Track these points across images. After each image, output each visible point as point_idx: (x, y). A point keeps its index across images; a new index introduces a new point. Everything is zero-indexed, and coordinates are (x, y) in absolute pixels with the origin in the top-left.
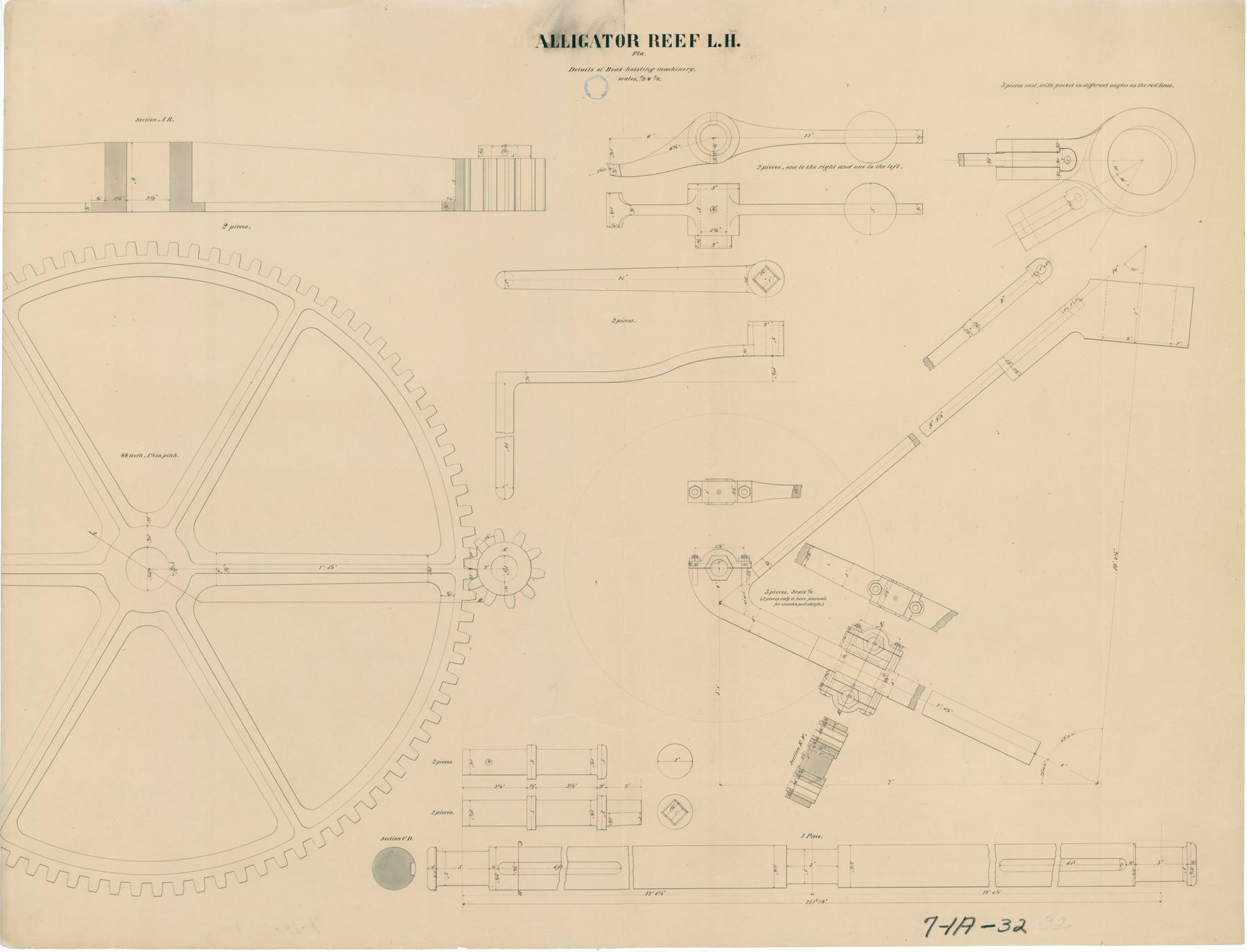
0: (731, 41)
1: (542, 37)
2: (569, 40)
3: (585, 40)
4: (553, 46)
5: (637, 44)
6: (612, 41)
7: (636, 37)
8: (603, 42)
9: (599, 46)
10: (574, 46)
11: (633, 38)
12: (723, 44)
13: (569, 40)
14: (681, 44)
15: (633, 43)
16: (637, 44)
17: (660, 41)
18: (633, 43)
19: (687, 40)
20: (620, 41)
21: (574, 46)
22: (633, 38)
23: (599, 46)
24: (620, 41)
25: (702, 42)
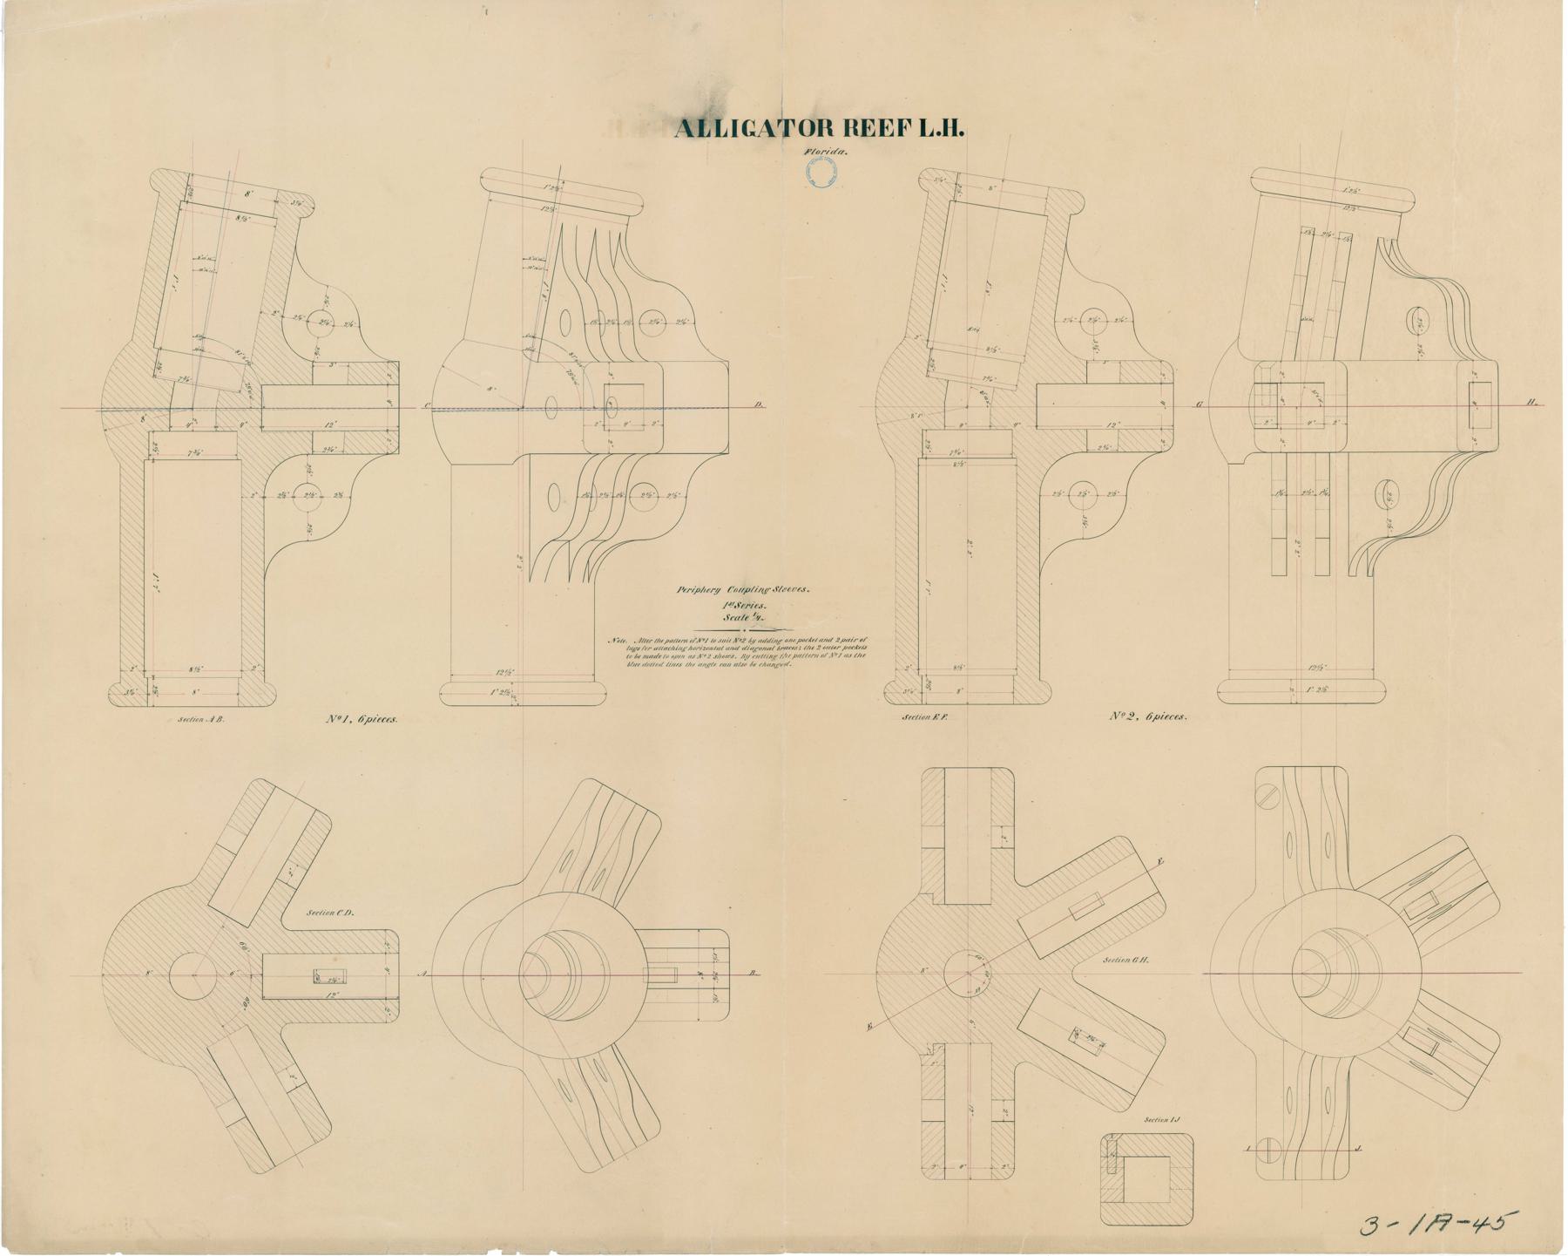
1: (685, 122)
3: (749, 125)
4: (701, 135)
5: (830, 133)
6: (794, 130)
7: (829, 123)
8: (779, 130)
9: (771, 134)
10: (735, 135)
11: (825, 124)
13: (726, 126)
15: (825, 131)
16: (830, 133)
17: (859, 128)
18: (825, 131)
21: (735, 135)
22: (825, 124)
23: (771, 134)
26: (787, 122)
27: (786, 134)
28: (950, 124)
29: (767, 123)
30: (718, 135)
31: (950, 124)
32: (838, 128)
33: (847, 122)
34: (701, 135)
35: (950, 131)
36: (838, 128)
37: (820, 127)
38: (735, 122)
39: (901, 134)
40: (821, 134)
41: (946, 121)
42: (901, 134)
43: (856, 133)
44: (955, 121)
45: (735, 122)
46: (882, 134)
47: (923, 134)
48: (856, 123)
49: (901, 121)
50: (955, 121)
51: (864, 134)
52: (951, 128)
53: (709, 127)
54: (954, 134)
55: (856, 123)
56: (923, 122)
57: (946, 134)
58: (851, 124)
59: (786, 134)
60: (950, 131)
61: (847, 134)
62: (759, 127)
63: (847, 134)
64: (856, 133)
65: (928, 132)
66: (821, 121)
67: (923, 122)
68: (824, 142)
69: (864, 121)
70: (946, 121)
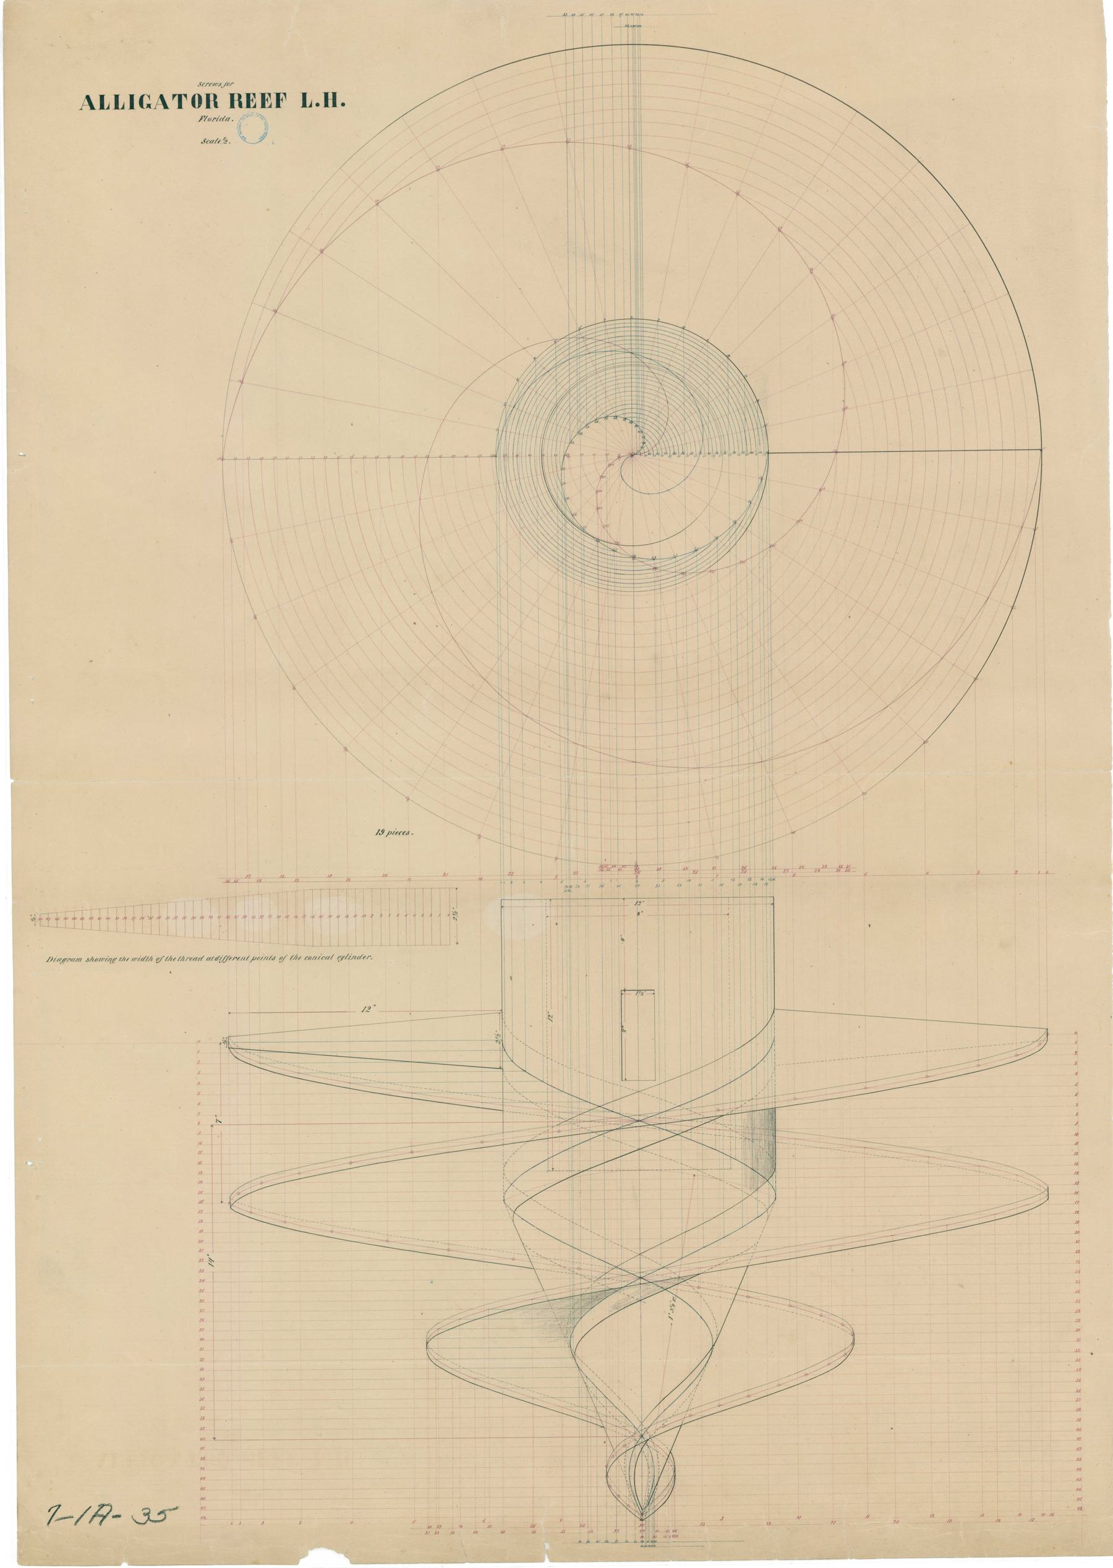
0: (330, 100)
1: (88, 97)
2: (124, 100)
3: (146, 101)
5: (216, 105)
6: (187, 103)
7: (215, 97)
8: (173, 104)
9: (166, 107)
10: (132, 107)
12: (322, 103)
13: (124, 100)
14: (267, 105)
17: (244, 100)
18: (212, 104)
19: (258, 100)
20: (196, 101)
21: (132, 107)
23: (166, 107)
24: (196, 101)
25: (292, 101)
26: (180, 96)
27: (180, 107)
28: (330, 96)
29: (162, 97)
30: (117, 107)
31: (330, 96)
32: (224, 101)
33: (232, 95)
34: (102, 107)
35: (330, 102)
36: (224, 101)
37: (211, 101)
38: (132, 97)
39: (278, 106)
40: (208, 106)
41: (326, 94)
42: (278, 106)
43: (240, 105)
44: (334, 94)
45: (132, 97)
46: (263, 106)
47: (304, 105)
48: (240, 96)
49: (278, 95)
50: (334, 94)
51: (248, 106)
52: (330, 100)
53: (109, 100)
54: (334, 105)
55: (240, 96)
56: (304, 95)
57: (326, 105)
58: (236, 97)
59: (180, 107)
60: (330, 102)
61: (232, 106)
62: (155, 100)
63: (232, 106)
64: (240, 105)
65: (308, 104)
66: (208, 96)
67: (304, 95)
68: (212, 112)
69: (248, 95)
70: (326, 94)
